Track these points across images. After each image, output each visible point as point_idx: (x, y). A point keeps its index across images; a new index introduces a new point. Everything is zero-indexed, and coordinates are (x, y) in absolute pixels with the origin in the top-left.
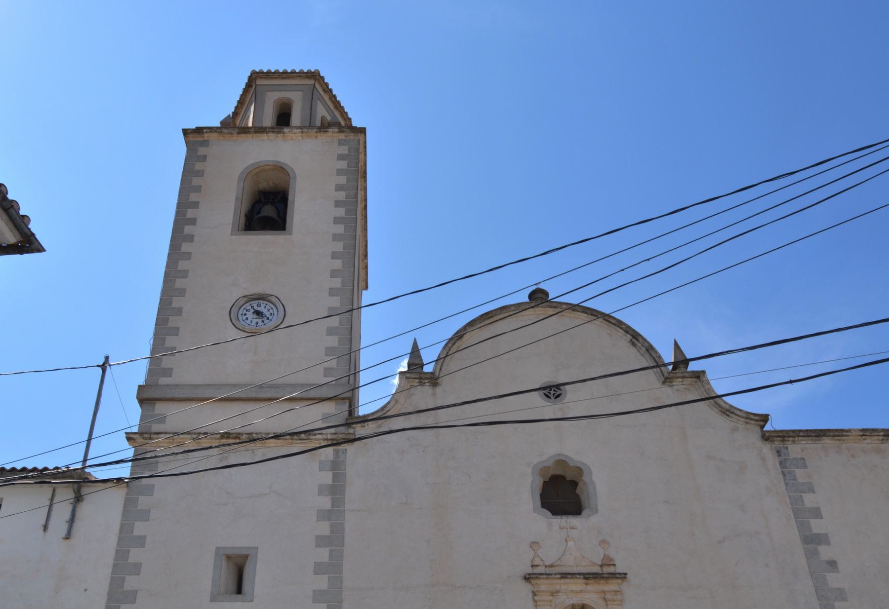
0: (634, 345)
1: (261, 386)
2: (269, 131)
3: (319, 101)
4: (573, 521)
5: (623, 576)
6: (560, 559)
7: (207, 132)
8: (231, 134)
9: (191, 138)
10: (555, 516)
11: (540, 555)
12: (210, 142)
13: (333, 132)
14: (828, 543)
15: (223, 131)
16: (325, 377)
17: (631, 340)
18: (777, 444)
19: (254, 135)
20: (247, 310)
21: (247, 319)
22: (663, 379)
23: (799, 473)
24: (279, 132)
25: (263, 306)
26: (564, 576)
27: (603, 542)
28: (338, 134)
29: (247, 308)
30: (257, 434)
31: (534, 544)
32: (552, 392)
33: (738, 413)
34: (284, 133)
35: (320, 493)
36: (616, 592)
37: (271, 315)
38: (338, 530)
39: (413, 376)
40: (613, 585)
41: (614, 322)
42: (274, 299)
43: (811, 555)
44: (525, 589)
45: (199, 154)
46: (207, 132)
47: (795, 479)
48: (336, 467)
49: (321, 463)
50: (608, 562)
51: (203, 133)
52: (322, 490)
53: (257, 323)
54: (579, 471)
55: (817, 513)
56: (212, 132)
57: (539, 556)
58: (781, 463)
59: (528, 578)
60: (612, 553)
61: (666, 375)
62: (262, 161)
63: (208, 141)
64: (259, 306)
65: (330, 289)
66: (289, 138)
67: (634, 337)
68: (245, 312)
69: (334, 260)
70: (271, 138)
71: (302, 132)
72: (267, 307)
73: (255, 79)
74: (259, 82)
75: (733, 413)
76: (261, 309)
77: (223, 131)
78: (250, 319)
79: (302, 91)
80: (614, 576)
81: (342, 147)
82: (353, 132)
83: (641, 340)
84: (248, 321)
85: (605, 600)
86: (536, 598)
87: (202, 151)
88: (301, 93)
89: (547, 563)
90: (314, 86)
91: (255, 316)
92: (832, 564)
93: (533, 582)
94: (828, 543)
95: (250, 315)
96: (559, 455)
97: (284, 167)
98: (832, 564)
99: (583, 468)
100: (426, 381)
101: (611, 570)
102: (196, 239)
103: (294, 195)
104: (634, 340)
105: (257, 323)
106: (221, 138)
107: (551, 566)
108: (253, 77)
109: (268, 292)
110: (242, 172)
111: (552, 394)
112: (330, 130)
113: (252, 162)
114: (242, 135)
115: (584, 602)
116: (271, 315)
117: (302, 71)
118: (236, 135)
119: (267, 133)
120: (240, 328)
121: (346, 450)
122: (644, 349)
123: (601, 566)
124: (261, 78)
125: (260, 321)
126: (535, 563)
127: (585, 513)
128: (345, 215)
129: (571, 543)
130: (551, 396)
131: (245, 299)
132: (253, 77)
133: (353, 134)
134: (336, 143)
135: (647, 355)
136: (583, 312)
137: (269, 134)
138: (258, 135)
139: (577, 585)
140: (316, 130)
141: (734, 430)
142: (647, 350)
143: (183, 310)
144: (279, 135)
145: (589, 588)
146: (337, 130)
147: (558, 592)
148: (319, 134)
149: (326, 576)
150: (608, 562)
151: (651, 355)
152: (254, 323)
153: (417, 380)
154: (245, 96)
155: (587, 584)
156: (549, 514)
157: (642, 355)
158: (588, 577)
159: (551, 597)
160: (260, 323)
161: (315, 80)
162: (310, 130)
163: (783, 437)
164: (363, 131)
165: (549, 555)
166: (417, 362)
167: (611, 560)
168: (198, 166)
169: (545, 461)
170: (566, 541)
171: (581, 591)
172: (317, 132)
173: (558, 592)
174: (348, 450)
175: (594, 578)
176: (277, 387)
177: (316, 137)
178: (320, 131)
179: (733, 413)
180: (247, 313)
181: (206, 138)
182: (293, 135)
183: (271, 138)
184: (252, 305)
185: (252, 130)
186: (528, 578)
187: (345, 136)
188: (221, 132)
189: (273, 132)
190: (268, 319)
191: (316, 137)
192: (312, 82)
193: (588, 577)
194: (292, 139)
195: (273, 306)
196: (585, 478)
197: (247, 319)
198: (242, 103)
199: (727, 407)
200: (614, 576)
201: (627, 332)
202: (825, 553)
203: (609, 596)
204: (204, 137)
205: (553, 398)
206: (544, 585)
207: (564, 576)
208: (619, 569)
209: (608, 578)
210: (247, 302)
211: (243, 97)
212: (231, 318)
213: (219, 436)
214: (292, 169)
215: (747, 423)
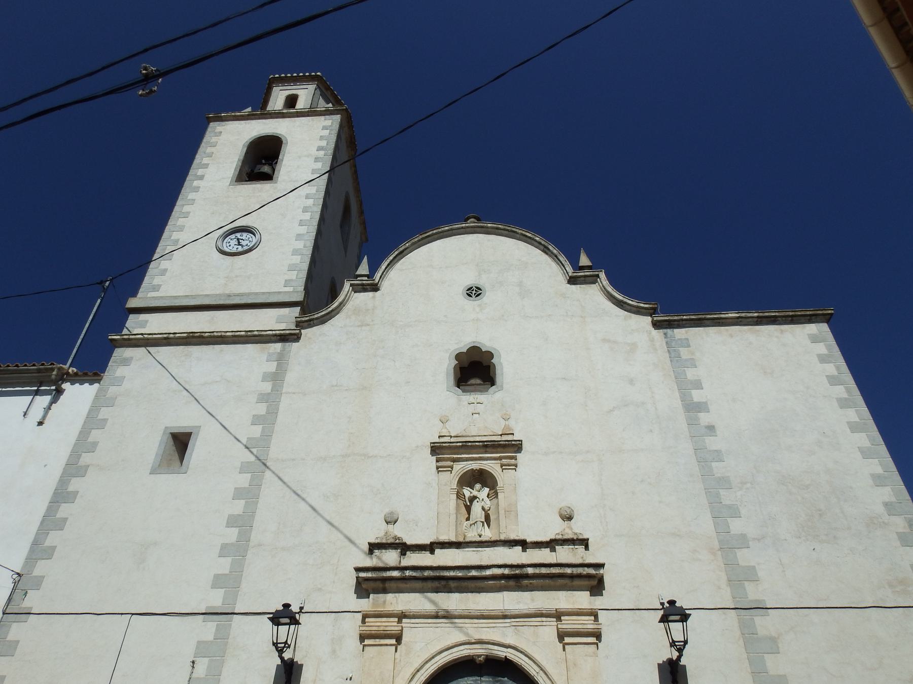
1: (229, 296)
6: (464, 430)
10: (465, 394)
11: (448, 427)
14: (708, 411)
32: (474, 292)
43: (692, 423)
45: (216, 131)
49: (270, 355)
52: (266, 377)
55: (698, 385)
57: (446, 428)
58: (667, 343)
60: (512, 423)
61: (570, 275)
68: (229, 240)
92: (711, 428)
94: (708, 411)
96: (474, 342)
111: (473, 294)
167: (510, 429)
169: (461, 348)
176: (242, 295)
180: (231, 241)
186: (436, 449)
195: (252, 235)
197: (230, 246)
202: (704, 418)
205: (474, 296)
214: (285, 138)
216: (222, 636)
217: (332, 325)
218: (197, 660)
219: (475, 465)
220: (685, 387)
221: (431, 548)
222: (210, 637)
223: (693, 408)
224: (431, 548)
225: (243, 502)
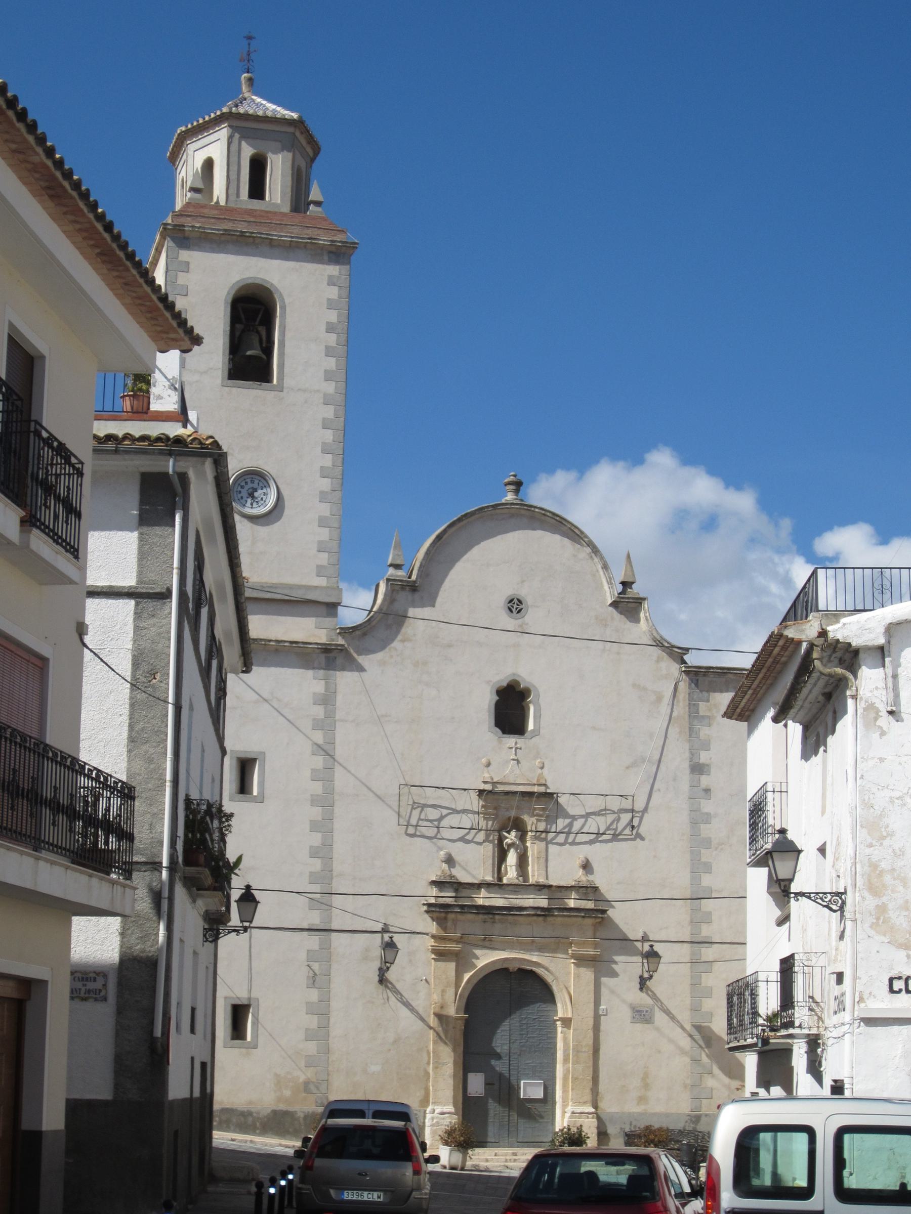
25: (256, 482)
29: (241, 484)
37: (264, 495)
64: (252, 482)
68: (239, 489)
92: (707, 791)
98: (707, 791)
100: (407, 587)
116: (264, 495)
174: (337, 659)
180: (242, 490)
184: (246, 481)
202: (705, 781)
216: (326, 947)
222: (317, 947)
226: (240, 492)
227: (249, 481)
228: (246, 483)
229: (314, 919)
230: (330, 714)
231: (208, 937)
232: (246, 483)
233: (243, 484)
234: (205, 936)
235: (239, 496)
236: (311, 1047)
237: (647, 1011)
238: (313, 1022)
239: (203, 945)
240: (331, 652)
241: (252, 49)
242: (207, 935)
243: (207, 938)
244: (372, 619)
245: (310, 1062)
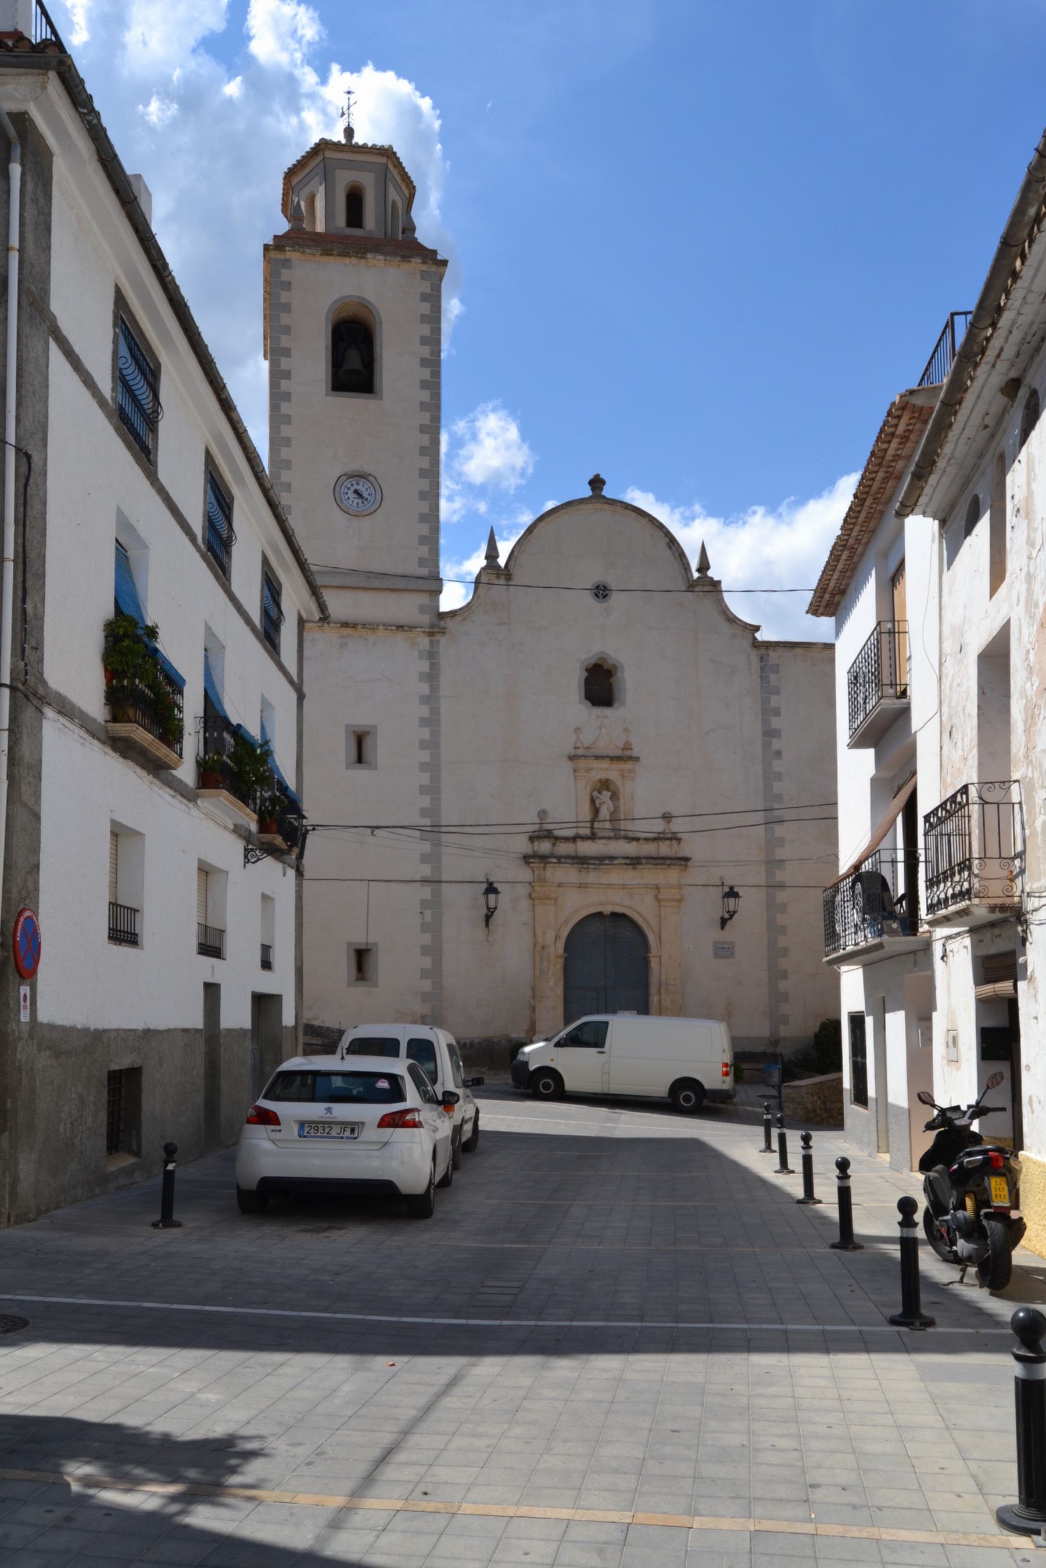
0: (670, 547)
2: (353, 256)
3: (390, 183)
4: (607, 711)
5: (637, 759)
7: (289, 251)
8: (314, 255)
9: (273, 255)
10: (594, 707)
12: (292, 262)
13: (416, 263)
14: (779, 737)
15: (306, 250)
16: (420, 566)
17: (668, 543)
18: (763, 651)
19: (337, 258)
20: (348, 489)
21: (349, 498)
22: (688, 585)
23: (772, 677)
24: (362, 258)
25: (361, 484)
26: (597, 757)
27: (626, 730)
28: (421, 265)
29: (348, 486)
30: (369, 624)
31: (578, 730)
33: (739, 623)
34: (367, 259)
35: (421, 680)
36: (631, 771)
38: (435, 712)
39: (493, 572)
40: (628, 766)
41: (657, 524)
42: (371, 479)
43: (767, 745)
44: (568, 766)
46: (289, 251)
47: (768, 682)
48: (432, 655)
50: (627, 747)
51: (285, 251)
53: (358, 504)
54: (615, 667)
55: (777, 712)
56: (295, 251)
58: (761, 668)
59: (572, 758)
61: (691, 583)
62: (347, 296)
63: (288, 260)
64: (358, 484)
65: (420, 469)
66: (371, 264)
67: (671, 541)
68: (346, 490)
69: (421, 435)
70: (353, 262)
71: (385, 260)
72: (366, 486)
73: (323, 150)
74: (329, 154)
75: (735, 622)
76: (360, 488)
77: (306, 250)
78: (351, 499)
79: (374, 172)
80: (630, 758)
81: (423, 281)
82: (436, 264)
83: (676, 546)
84: (350, 502)
85: (623, 776)
86: (576, 774)
87: (285, 274)
88: (373, 174)
89: (586, 746)
90: (387, 167)
91: (355, 496)
93: (575, 761)
94: (779, 737)
95: (351, 494)
97: (369, 306)
98: (779, 753)
99: (618, 665)
101: (628, 753)
102: (294, 398)
103: (381, 346)
104: (670, 544)
105: (358, 504)
106: (303, 258)
107: (588, 748)
108: (322, 146)
109: (367, 468)
110: (329, 311)
112: (413, 260)
113: (337, 296)
114: (325, 257)
115: (608, 777)
117: (374, 147)
118: (318, 256)
119: (350, 257)
120: (345, 510)
121: (439, 641)
122: (677, 554)
123: (623, 749)
124: (329, 149)
125: (360, 501)
126: (578, 746)
127: (616, 705)
128: (431, 378)
129: (603, 730)
130: (600, 595)
131: (346, 477)
132: (322, 146)
133: (435, 266)
134: (419, 276)
135: (679, 560)
136: (633, 511)
137: (352, 259)
138: (341, 258)
139: (604, 764)
140: (399, 259)
141: (734, 636)
142: (680, 555)
143: (293, 485)
144: (362, 260)
145: (612, 766)
146: (420, 261)
147: (591, 769)
148: (401, 264)
149: (429, 751)
150: (627, 747)
151: (682, 560)
152: (355, 504)
153: (495, 575)
154: (308, 160)
155: (611, 763)
156: (589, 704)
157: (675, 558)
158: (613, 759)
159: (587, 774)
160: (361, 504)
161: (388, 157)
162: (393, 259)
163: (767, 646)
164: (444, 263)
165: (587, 738)
166: (494, 554)
167: (631, 745)
168: (284, 297)
170: (600, 728)
171: (607, 769)
172: (400, 261)
173: (591, 769)
175: (618, 760)
177: (398, 266)
178: (403, 261)
179: (735, 622)
180: (348, 491)
181: (288, 257)
182: (376, 261)
183: (353, 262)
185: (336, 253)
186: (572, 758)
187: (428, 268)
188: (304, 252)
189: (356, 257)
190: (367, 500)
191: (398, 266)
192: (384, 160)
193: (613, 759)
194: (374, 266)
195: (370, 485)
196: (619, 675)
198: (302, 165)
199: (732, 617)
200: (630, 758)
201: (666, 536)
203: (626, 774)
204: (285, 255)
206: (582, 764)
207: (597, 757)
208: (635, 753)
209: (626, 761)
210: (347, 479)
211: (306, 160)
212: (335, 499)
213: (339, 625)
215: (744, 631)
216: (436, 895)
217: (473, 621)
218: (424, 911)
219: (603, 776)
220: (768, 712)
221: (574, 839)
222: (429, 897)
223: (770, 733)
224: (574, 839)
225: (428, 797)
226: (347, 493)
227: (354, 483)
228: (352, 485)
229: (426, 871)
230: (434, 688)
231: (250, 858)
232: (352, 485)
233: (349, 485)
234: (246, 856)
235: (346, 497)
236: (427, 985)
237: (728, 948)
238: (427, 962)
239: (245, 866)
240: (434, 636)
241: (351, 103)
242: (249, 855)
243: (249, 860)
244: (471, 605)
245: (425, 997)
